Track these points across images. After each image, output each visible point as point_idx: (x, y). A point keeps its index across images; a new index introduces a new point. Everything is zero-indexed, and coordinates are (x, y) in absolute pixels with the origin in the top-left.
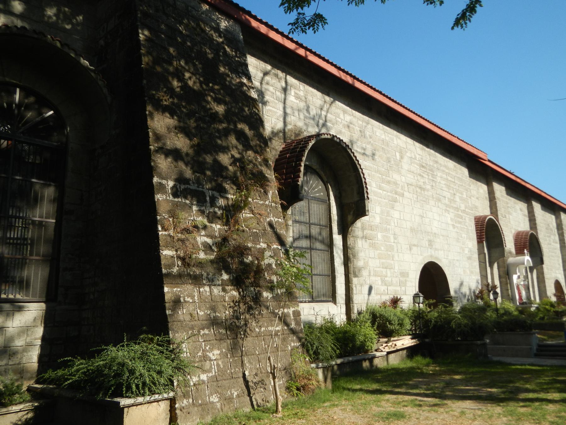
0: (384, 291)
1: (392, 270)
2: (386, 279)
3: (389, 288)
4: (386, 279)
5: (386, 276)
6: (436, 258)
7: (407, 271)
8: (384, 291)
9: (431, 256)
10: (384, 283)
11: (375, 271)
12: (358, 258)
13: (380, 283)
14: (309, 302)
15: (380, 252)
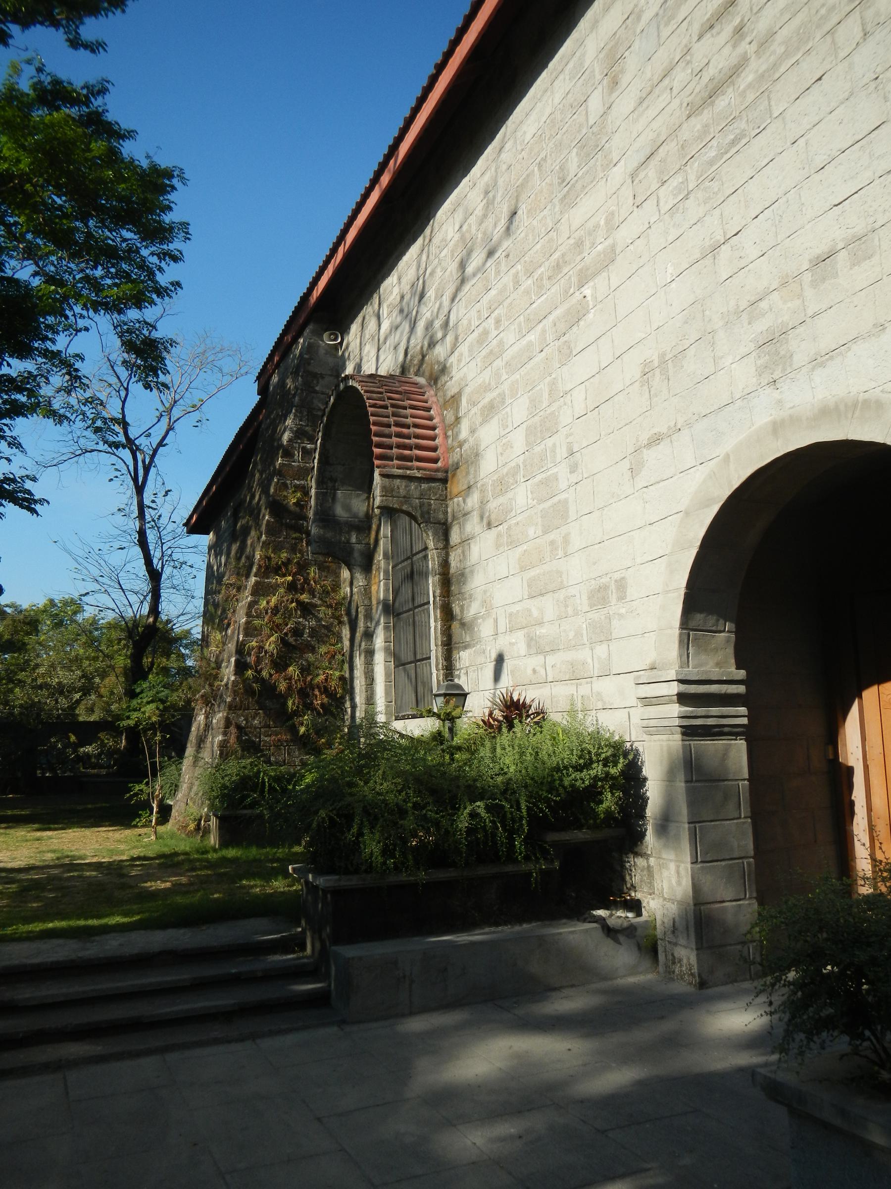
0: (534, 671)
1: (561, 594)
2: (542, 631)
3: (551, 660)
4: (542, 631)
5: (541, 624)
6: (826, 412)
7: (617, 576)
8: (534, 671)
9: (776, 428)
10: (536, 647)
11: (511, 615)
12: (471, 596)
13: (522, 648)
14: (414, 717)
15: (525, 547)
